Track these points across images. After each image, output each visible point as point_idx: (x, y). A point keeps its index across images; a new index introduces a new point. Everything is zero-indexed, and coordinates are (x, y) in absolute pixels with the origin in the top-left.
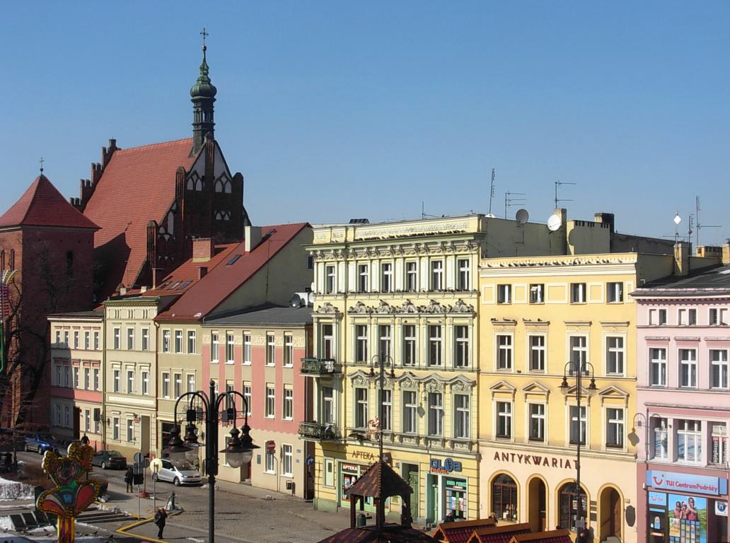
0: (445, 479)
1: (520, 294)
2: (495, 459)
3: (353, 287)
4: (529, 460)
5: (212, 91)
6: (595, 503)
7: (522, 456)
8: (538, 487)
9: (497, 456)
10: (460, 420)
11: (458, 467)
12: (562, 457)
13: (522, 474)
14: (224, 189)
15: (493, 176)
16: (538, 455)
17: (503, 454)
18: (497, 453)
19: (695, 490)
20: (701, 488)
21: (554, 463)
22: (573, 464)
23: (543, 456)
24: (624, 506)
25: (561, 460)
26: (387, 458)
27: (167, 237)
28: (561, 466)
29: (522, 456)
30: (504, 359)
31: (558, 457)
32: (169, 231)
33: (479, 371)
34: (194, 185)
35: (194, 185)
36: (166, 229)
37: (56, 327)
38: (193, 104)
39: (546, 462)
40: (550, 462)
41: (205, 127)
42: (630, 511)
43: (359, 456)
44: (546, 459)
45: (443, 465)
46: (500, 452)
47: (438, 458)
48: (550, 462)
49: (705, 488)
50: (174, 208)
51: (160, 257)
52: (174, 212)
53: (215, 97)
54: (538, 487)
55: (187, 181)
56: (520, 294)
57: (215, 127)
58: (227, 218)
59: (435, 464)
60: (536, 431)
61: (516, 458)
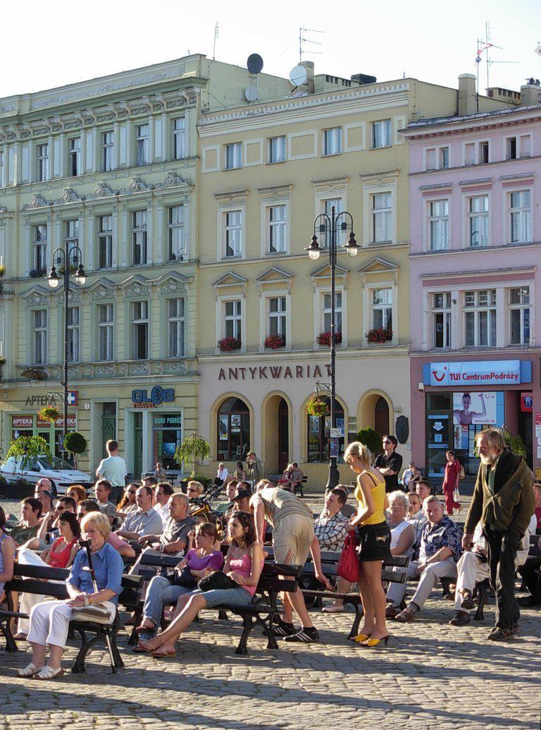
0: (155, 415)
3: (28, 176)
4: (266, 373)
9: (222, 374)
10: (175, 333)
11: (169, 395)
13: (256, 393)
15: (216, 32)
16: (276, 365)
18: (222, 370)
19: (489, 382)
20: (497, 377)
21: (299, 373)
22: (324, 371)
23: (284, 365)
24: (393, 418)
25: (308, 366)
26: (73, 398)
29: (255, 368)
31: (304, 365)
33: (198, 262)
39: (288, 372)
42: (402, 421)
43: (35, 403)
45: (149, 397)
46: (226, 368)
47: (142, 388)
49: (502, 376)
54: (281, 408)
59: (139, 397)
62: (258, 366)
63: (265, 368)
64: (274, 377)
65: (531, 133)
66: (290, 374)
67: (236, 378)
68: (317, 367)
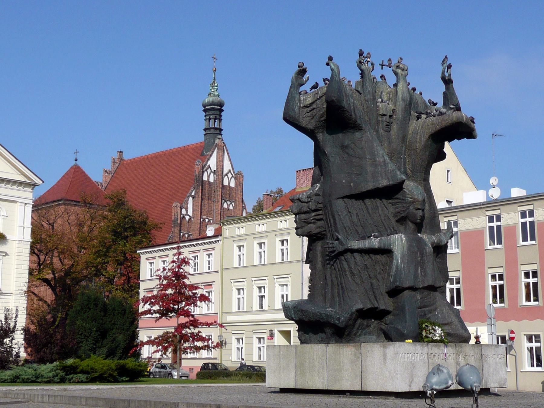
5: (221, 105)
14: (229, 183)
27: (187, 218)
32: (189, 213)
34: (209, 176)
35: (209, 176)
36: (187, 211)
37: (148, 259)
38: (204, 114)
41: (214, 132)
50: (193, 194)
51: (182, 234)
52: (193, 197)
53: (223, 108)
55: (203, 173)
57: (222, 132)
58: (231, 207)
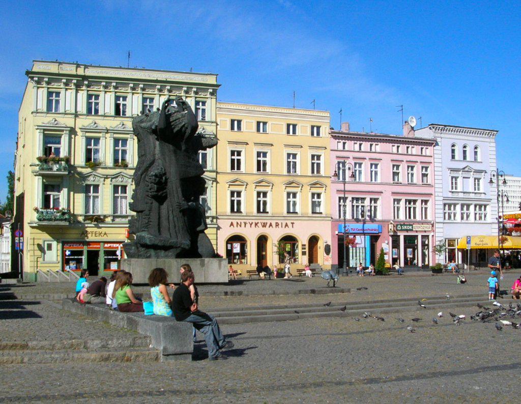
1: (249, 125)
2: (230, 226)
3: (82, 108)
6: (305, 245)
7: (252, 223)
8: (262, 241)
9: (232, 224)
12: (282, 221)
16: (265, 221)
17: (237, 223)
25: (282, 223)
28: (282, 227)
29: (252, 223)
30: (235, 165)
39: (271, 225)
40: (274, 225)
44: (271, 224)
46: (235, 222)
48: (274, 225)
49: (372, 230)
54: (262, 241)
56: (249, 125)
60: (261, 208)
61: (248, 225)
62: (254, 221)
63: (258, 223)
64: (263, 227)
65: (415, 146)
66: (272, 226)
67: (240, 226)
68: (286, 223)
